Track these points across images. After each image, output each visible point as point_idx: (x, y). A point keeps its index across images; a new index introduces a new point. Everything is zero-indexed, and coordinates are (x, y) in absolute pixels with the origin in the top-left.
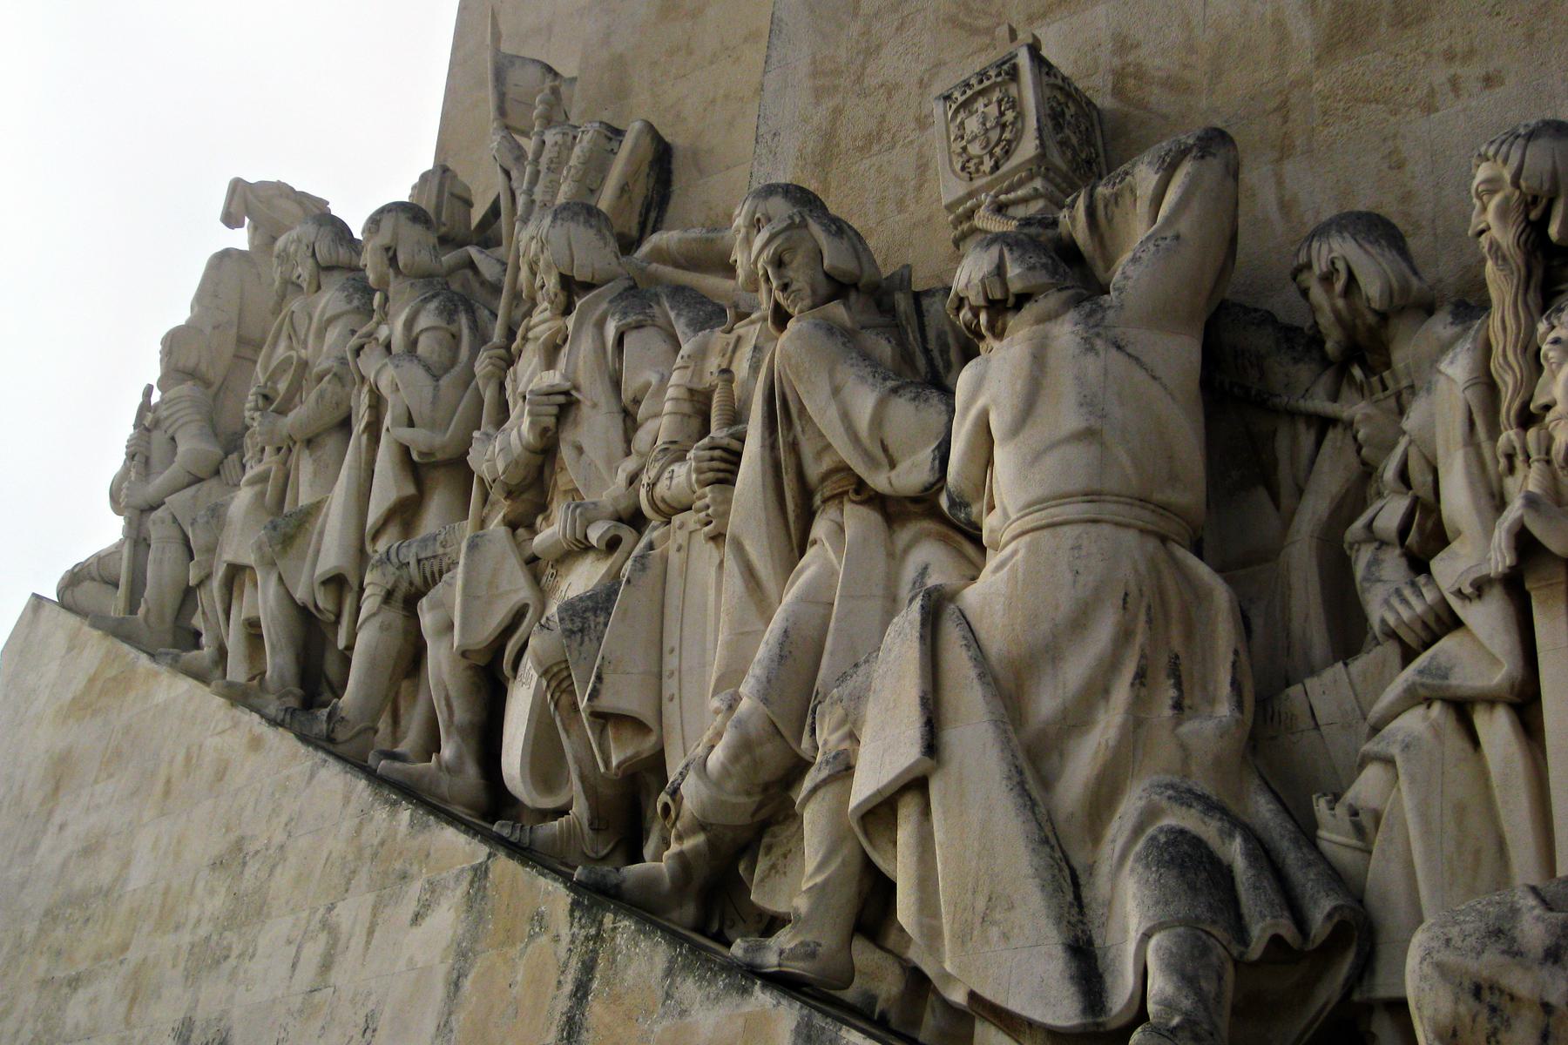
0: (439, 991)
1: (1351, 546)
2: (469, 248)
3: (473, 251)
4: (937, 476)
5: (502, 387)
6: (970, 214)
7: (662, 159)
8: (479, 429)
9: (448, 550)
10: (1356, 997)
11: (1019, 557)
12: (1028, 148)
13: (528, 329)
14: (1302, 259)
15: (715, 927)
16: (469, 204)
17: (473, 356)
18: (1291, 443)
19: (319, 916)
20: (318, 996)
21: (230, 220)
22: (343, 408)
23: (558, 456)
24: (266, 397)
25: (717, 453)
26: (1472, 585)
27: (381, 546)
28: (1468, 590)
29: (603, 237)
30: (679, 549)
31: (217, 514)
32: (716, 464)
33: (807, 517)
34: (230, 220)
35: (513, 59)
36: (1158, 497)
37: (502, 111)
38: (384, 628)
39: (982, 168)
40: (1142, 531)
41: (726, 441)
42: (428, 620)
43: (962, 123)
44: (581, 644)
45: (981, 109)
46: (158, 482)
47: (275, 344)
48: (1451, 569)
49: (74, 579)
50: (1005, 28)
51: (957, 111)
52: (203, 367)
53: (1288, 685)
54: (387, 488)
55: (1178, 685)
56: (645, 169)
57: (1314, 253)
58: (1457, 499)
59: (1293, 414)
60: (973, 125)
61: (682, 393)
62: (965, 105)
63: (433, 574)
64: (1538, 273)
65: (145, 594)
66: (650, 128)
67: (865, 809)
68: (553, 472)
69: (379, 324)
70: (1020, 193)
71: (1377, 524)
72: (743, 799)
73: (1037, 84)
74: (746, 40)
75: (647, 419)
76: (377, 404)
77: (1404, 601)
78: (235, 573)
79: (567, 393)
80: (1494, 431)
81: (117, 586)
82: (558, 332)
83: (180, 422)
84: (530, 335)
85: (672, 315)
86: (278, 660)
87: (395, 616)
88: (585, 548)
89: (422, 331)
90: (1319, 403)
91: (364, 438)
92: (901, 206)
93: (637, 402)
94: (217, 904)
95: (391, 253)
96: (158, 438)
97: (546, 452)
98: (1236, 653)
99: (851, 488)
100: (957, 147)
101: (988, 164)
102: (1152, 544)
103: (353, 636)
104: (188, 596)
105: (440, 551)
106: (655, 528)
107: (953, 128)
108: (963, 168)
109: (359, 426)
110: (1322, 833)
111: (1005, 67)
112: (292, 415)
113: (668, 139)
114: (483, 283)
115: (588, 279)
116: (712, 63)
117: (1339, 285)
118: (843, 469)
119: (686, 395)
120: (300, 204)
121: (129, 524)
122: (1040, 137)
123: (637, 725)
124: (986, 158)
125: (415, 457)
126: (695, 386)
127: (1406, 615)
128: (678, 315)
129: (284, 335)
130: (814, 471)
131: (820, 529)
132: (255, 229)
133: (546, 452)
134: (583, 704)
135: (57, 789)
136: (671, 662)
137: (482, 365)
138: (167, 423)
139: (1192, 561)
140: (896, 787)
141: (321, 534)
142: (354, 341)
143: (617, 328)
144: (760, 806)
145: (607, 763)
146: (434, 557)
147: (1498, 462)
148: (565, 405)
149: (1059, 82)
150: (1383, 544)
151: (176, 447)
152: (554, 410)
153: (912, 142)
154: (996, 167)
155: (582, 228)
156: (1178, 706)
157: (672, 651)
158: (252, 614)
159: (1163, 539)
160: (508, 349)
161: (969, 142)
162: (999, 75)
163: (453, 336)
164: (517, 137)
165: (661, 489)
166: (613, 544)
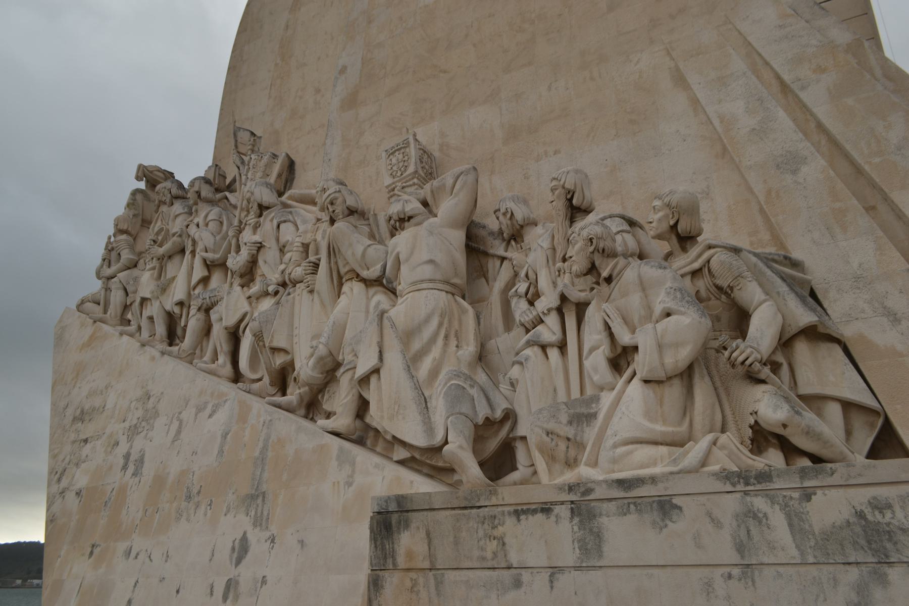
0: (219, 439)
1: (510, 297)
3: (227, 194)
4: (382, 273)
5: (238, 240)
6: (393, 190)
7: (291, 166)
8: (230, 253)
9: (220, 294)
10: (511, 436)
11: (408, 300)
13: (247, 221)
14: (497, 208)
16: (225, 178)
18: (492, 265)
19: (176, 416)
20: (176, 443)
21: (138, 178)
23: (258, 264)
24: (154, 241)
26: (547, 310)
27: (197, 291)
28: (546, 312)
29: (272, 192)
31: (136, 280)
32: (311, 268)
33: (341, 285)
34: (138, 178)
35: (240, 128)
37: (236, 146)
38: (198, 320)
39: (397, 174)
40: (447, 292)
41: (314, 260)
43: (391, 160)
44: (266, 325)
45: (397, 155)
46: (114, 268)
47: (156, 223)
48: (542, 304)
50: (405, 129)
51: (389, 156)
52: (130, 229)
53: (491, 339)
54: (199, 272)
55: (458, 340)
56: (286, 169)
57: (501, 206)
59: (494, 256)
60: (394, 161)
61: (299, 244)
62: (392, 154)
63: (214, 301)
64: (569, 215)
65: (110, 307)
66: (287, 155)
67: (360, 379)
68: (256, 269)
69: (194, 217)
70: (408, 184)
72: (321, 376)
73: (415, 148)
74: (319, 127)
75: (289, 252)
76: (194, 243)
77: (527, 315)
78: (144, 300)
79: (261, 243)
80: (554, 264)
81: (99, 304)
82: (258, 222)
83: (123, 248)
86: (161, 329)
87: (201, 316)
88: (267, 294)
89: (210, 221)
90: (501, 252)
91: (190, 256)
93: (284, 247)
94: (139, 413)
95: (198, 194)
96: (114, 254)
97: (253, 263)
98: (475, 330)
99: (355, 276)
100: (389, 167)
101: (399, 173)
102: (450, 296)
103: (187, 322)
104: (126, 307)
105: (217, 294)
106: (290, 288)
108: (391, 174)
109: (187, 253)
110: (500, 385)
111: (405, 142)
112: (163, 247)
113: (293, 159)
114: (231, 204)
115: (268, 206)
116: (308, 134)
117: (509, 216)
118: (353, 271)
120: (164, 173)
123: (286, 351)
124: (399, 171)
125: (208, 263)
126: (304, 242)
127: (527, 319)
129: (159, 220)
130: (343, 270)
131: (346, 288)
132: (147, 181)
133: (253, 263)
134: (267, 345)
136: (296, 332)
137: (231, 233)
138: (117, 249)
139: (462, 301)
140: (369, 372)
141: (175, 288)
142: (186, 223)
143: (278, 222)
144: (326, 377)
146: (215, 296)
147: (555, 273)
148: (260, 247)
149: (422, 147)
150: (520, 297)
152: (256, 248)
153: (374, 164)
154: (402, 174)
156: (457, 346)
157: (296, 328)
159: (453, 295)
160: (240, 228)
162: (403, 144)
163: (221, 222)
164: (241, 155)
165: (292, 276)
166: (276, 293)
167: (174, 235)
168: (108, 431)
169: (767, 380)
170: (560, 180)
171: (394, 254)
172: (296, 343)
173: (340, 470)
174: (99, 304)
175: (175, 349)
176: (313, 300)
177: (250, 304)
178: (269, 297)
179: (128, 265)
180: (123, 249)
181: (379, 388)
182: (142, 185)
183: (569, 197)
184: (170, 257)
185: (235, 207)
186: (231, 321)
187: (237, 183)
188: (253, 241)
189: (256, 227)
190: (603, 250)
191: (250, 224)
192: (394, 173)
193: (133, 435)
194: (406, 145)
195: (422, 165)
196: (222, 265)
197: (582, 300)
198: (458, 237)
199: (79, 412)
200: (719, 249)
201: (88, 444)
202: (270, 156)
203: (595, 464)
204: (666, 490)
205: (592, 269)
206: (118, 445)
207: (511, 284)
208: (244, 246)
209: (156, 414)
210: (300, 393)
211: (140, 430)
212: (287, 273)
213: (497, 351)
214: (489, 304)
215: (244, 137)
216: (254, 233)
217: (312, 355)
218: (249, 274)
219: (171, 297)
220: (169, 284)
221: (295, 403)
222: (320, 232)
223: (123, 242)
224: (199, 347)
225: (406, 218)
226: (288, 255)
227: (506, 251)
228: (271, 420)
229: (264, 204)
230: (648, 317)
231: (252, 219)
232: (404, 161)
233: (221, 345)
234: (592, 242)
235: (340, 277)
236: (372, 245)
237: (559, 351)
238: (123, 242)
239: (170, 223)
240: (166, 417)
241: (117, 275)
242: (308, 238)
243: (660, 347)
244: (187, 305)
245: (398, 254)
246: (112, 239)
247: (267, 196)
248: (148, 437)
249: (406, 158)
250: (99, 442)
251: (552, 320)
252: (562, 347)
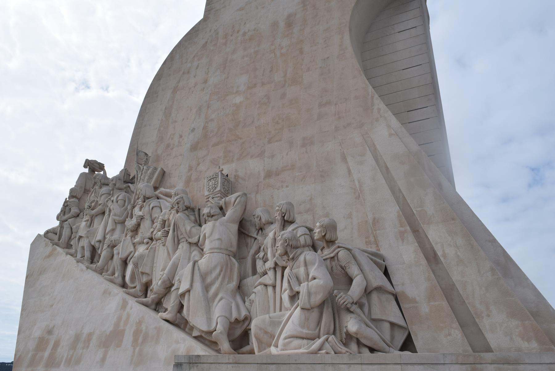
2: (129, 184)
5: (132, 211)
6: (208, 198)
8: (127, 218)
10: (248, 328)
11: (207, 257)
17: (128, 205)
21: (85, 166)
24: (89, 206)
26: (269, 268)
28: (268, 269)
32: (165, 234)
33: (179, 244)
34: (85, 166)
35: (140, 151)
36: (229, 249)
40: (226, 254)
41: (167, 230)
42: (115, 252)
43: (209, 183)
47: (92, 194)
49: (47, 232)
50: (218, 166)
52: (77, 196)
53: (245, 279)
59: (251, 237)
60: (210, 184)
61: (161, 220)
65: (62, 237)
66: (162, 169)
68: (139, 229)
69: (111, 197)
70: (216, 196)
71: (260, 256)
72: (162, 290)
73: (221, 178)
76: (110, 211)
78: (81, 237)
79: (143, 216)
81: (56, 234)
83: (73, 206)
84: (138, 203)
86: (87, 254)
90: (255, 236)
91: (107, 216)
92: (200, 191)
93: (154, 219)
97: (138, 225)
100: (208, 186)
101: (212, 191)
102: (227, 256)
104: (70, 238)
108: (208, 190)
109: (106, 214)
111: (217, 174)
113: (165, 170)
114: (131, 190)
119: (162, 221)
120: (99, 165)
121: (60, 223)
122: (220, 187)
125: (116, 221)
126: (163, 219)
129: (94, 192)
130: (180, 237)
131: (180, 246)
132: (90, 168)
133: (138, 225)
136: (155, 265)
137: (129, 207)
138: (70, 206)
139: (233, 259)
140: (185, 291)
142: (106, 200)
148: (142, 218)
150: (260, 259)
151: (71, 210)
154: (213, 191)
158: (83, 245)
159: (229, 255)
160: (134, 204)
161: (210, 186)
166: (148, 243)
167: (100, 205)
169: (354, 312)
170: (280, 207)
171: (203, 233)
174: (56, 234)
175: (94, 266)
177: (134, 247)
178: (144, 244)
179: (74, 215)
180: (73, 206)
181: (189, 300)
182: (86, 170)
183: (283, 215)
184: (96, 216)
185: (133, 192)
186: (124, 256)
187: (136, 179)
188: (139, 215)
189: (141, 208)
190: (291, 245)
191: (139, 204)
192: (210, 190)
194: (217, 177)
195: (224, 187)
197: (284, 266)
198: (235, 227)
200: (341, 248)
202: (153, 168)
203: (276, 346)
204: (296, 361)
205: (286, 253)
207: (258, 251)
208: (135, 216)
215: (142, 155)
216: (140, 210)
217: (160, 279)
218: (136, 229)
219: (94, 239)
221: (150, 302)
222: (172, 215)
223: (73, 203)
224: (107, 265)
225: (211, 216)
226: (155, 224)
227: (257, 235)
229: (147, 196)
230: (307, 279)
231: (140, 201)
232: (215, 184)
233: (118, 268)
234: (286, 241)
235: (179, 240)
236: (194, 226)
237: (273, 288)
238: (73, 203)
239: (99, 198)
241: (68, 220)
242: (166, 217)
243: (309, 294)
246: (68, 199)
247: (149, 192)
249: (216, 183)
251: (271, 273)
252: (274, 287)
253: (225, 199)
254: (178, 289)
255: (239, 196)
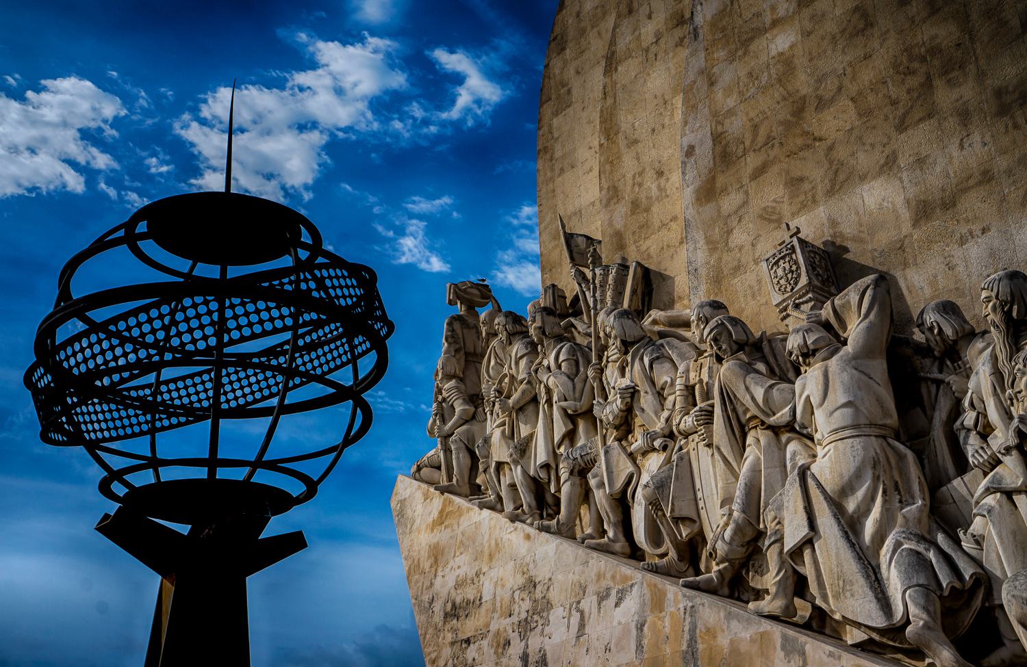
0: (634, 632)
3: (572, 320)
5: (601, 380)
6: (785, 309)
11: (832, 450)
12: (804, 280)
13: (608, 358)
15: (736, 595)
19: (574, 606)
20: (582, 639)
22: (533, 394)
24: (499, 392)
25: (703, 413)
27: (562, 449)
30: (694, 449)
33: (744, 435)
40: (875, 436)
42: (593, 482)
54: (560, 429)
55: (899, 493)
56: (640, 280)
58: (993, 415)
59: (926, 379)
60: (780, 272)
62: (776, 263)
66: (638, 264)
68: (632, 419)
69: (543, 359)
74: (671, 220)
77: (981, 456)
78: (500, 466)
79: (633, 388)
81: (439, 468)
85: (670, 352)
86: (526, 498)
90: (937, 375)
91: (546, 406)
93: (663, 389)
94: (527, 605)
98: (919, 478)
100: (775, 281)
101: (789, 289)
102: (880, 440)
105: (590, 451)
107: (772, 272)
108: (779, 290)
110: (962, 543)
111: (789, 246)
115: (633, 340)
120: (478, 289)
123: (692, 521)
125: (569, 412)
128: (672, 352)
131: (750, 440)
135: (436, 560)
136: (699, 495)
137: (590, 373)
139: (897, 444)
145: (681, 536)
148: (632, 393)
149: (811, 249)
155: (626, 320)
156: (901, 502)
159: (884, 437)
165: (682, 426)
166: (665, 448)
167: (522, 382)
168: (493, 627)
171: (804, 397)
172: (702, 508)
173: (789, 662)
176: (713, 455)
192: (783, 289)
193: (526, 632)
196: (588, 414)
199: (449, 606)
201: (471, 645)
206: (509, 644)
208: (612, 391)
209: (549, 605)
210: (719, 571)
211: (533, 625)
212: (674, 423)
213: (951, 501)
214: (931, 441)
216: (623, 375)
220: (527, 444)
225: (811, 352)
228: (693, 607)
240: (562, 608)
244: (554, 466)
245: (808, 397)
248: (545, 633)
250: (485, 643)
253: (833, 303)
254: (780, 540)
255: (868, 287)
